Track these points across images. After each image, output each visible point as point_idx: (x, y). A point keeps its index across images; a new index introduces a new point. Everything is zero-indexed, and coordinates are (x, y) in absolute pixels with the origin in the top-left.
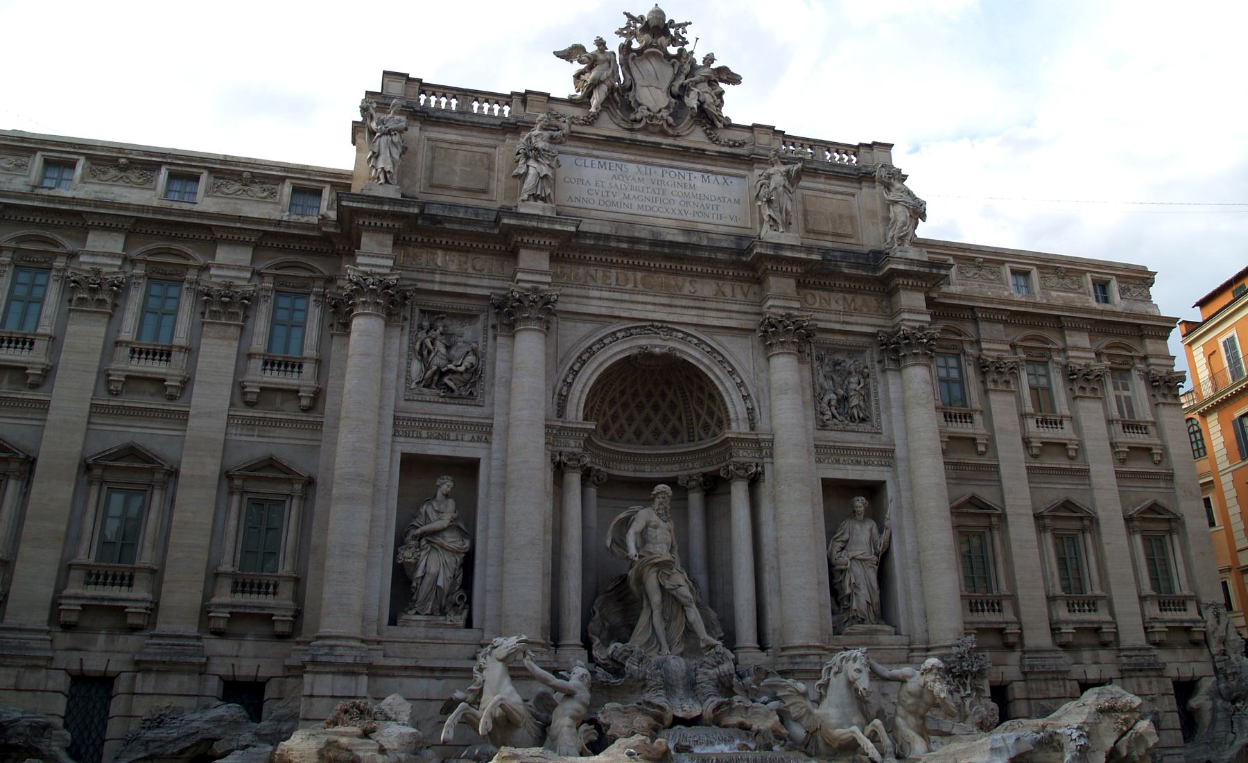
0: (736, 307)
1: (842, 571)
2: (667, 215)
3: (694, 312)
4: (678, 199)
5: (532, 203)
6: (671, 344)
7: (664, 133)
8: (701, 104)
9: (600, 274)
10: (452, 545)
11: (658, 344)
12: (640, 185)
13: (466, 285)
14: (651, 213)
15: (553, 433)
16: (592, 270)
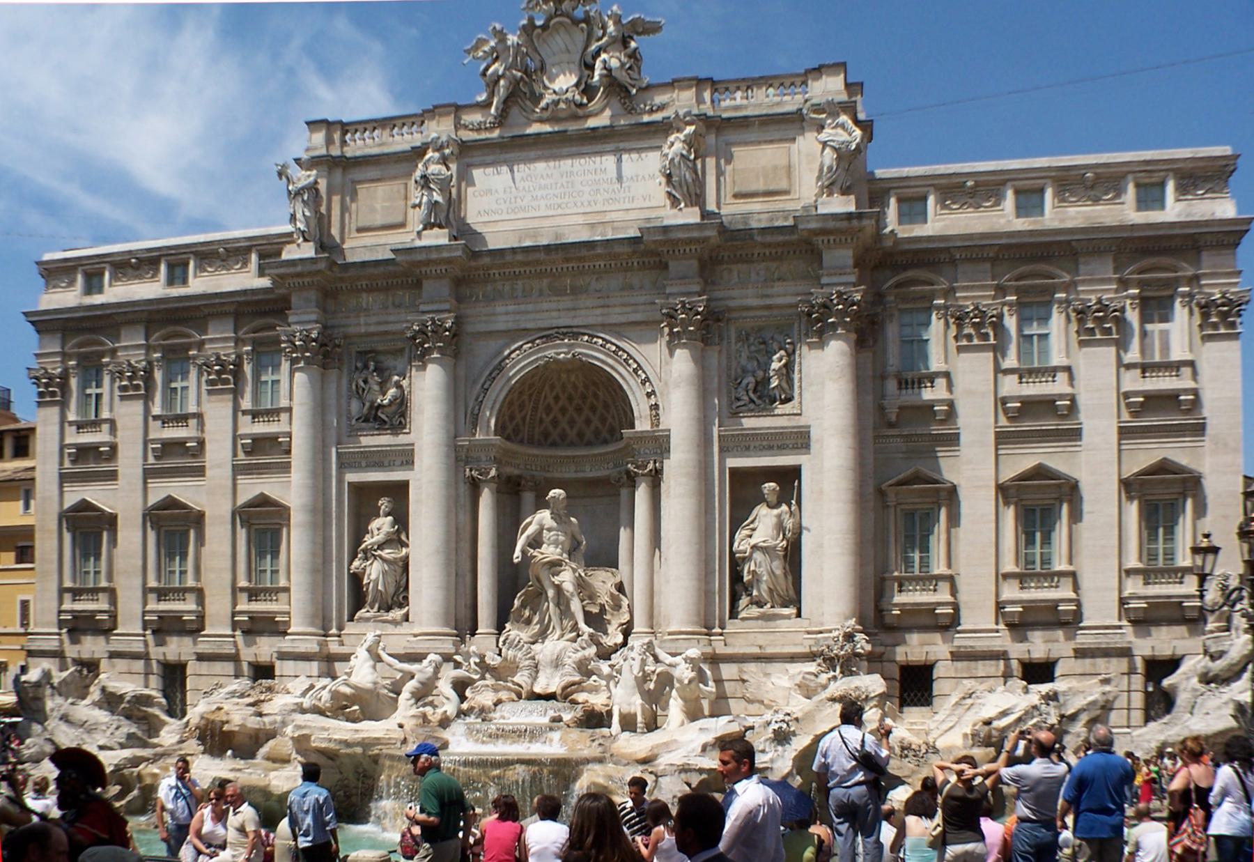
0: (642, 299)
1: (744, 559)
2: (575, 210)
3: (599, 311)
4: (587, 189)
7: (575, 117)
9: (507, 288)
10: (387, 556)
11: (559, 352)
13: (387, 323)
14: (560, 211)
16: (499, 285)
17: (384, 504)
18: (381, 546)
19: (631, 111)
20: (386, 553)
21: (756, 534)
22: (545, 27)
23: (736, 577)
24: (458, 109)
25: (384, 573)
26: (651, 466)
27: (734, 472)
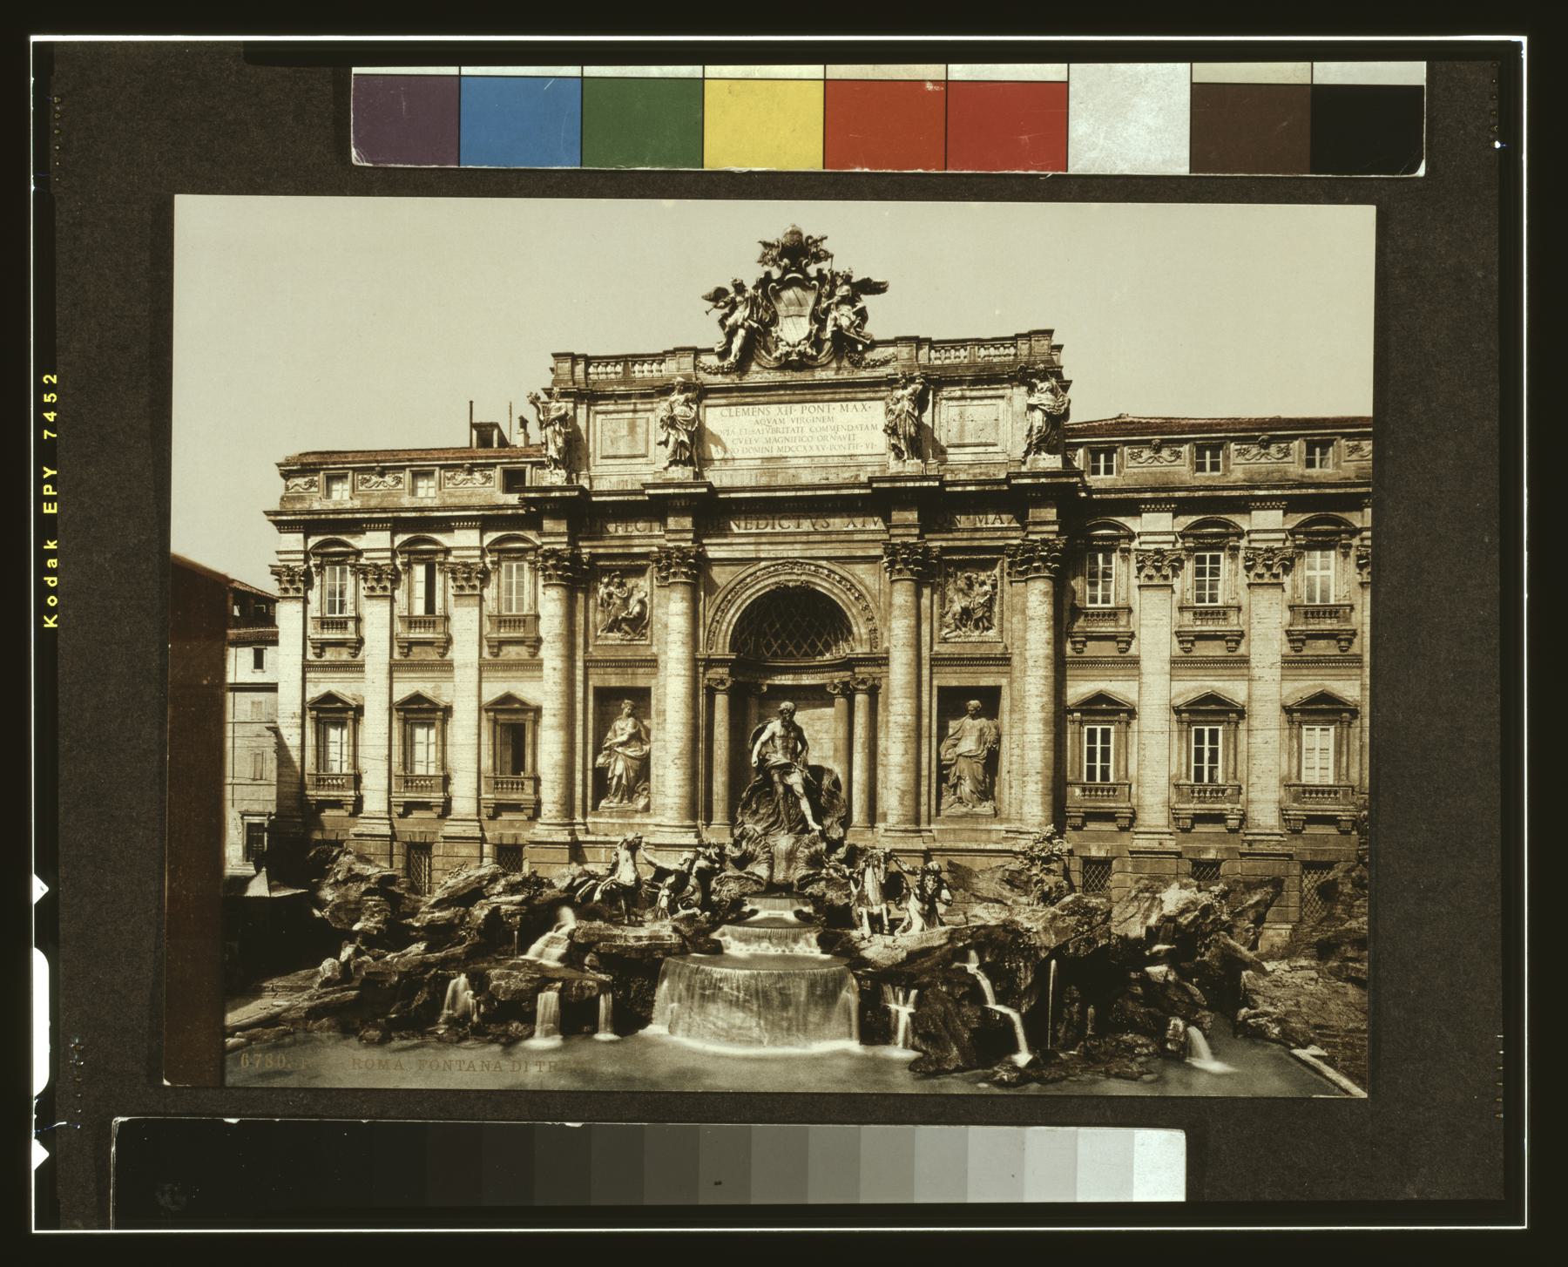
1: (949, 767)
5: (673, 468)
6: (804, 578)
8: (839, 333)
11: (793, 579)
12: (780, 426)
15: (698, 664)
17: (626, 706)
18: (622, 744)
19: (856, 364)
20: (629, 752)
21: (962, 743)
22: (779, 281)
23: (942, 778)
24: (697, 352)
25: (627, 769)
26: (870, 683)
27: (940, 689)
